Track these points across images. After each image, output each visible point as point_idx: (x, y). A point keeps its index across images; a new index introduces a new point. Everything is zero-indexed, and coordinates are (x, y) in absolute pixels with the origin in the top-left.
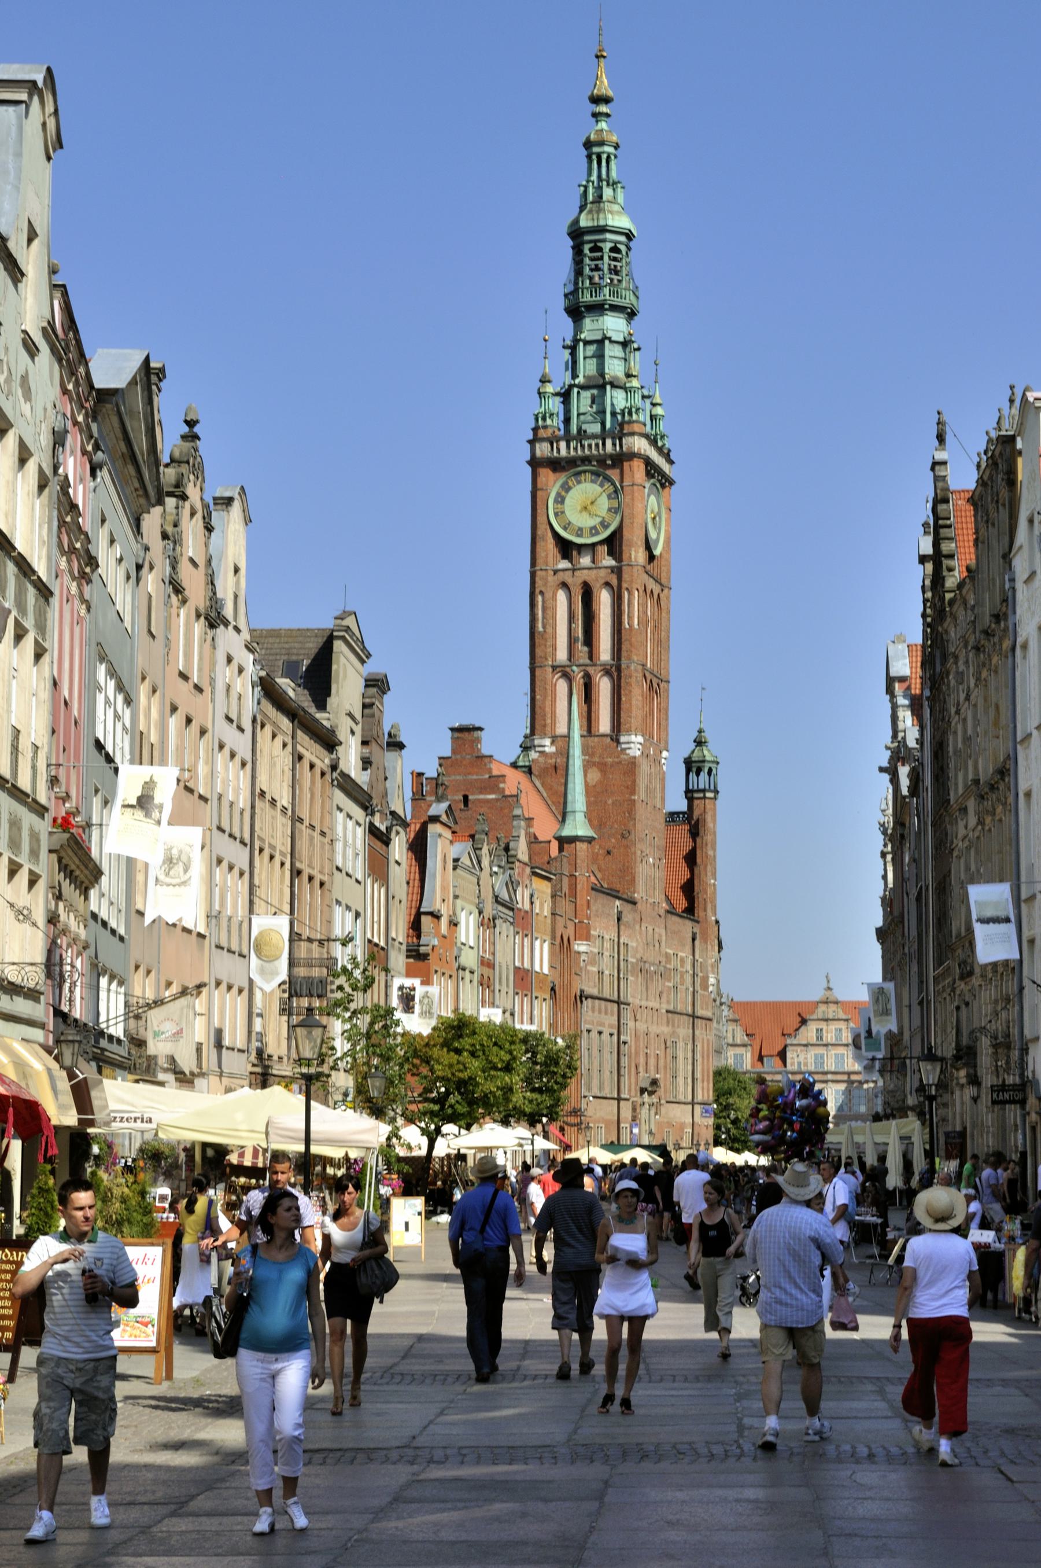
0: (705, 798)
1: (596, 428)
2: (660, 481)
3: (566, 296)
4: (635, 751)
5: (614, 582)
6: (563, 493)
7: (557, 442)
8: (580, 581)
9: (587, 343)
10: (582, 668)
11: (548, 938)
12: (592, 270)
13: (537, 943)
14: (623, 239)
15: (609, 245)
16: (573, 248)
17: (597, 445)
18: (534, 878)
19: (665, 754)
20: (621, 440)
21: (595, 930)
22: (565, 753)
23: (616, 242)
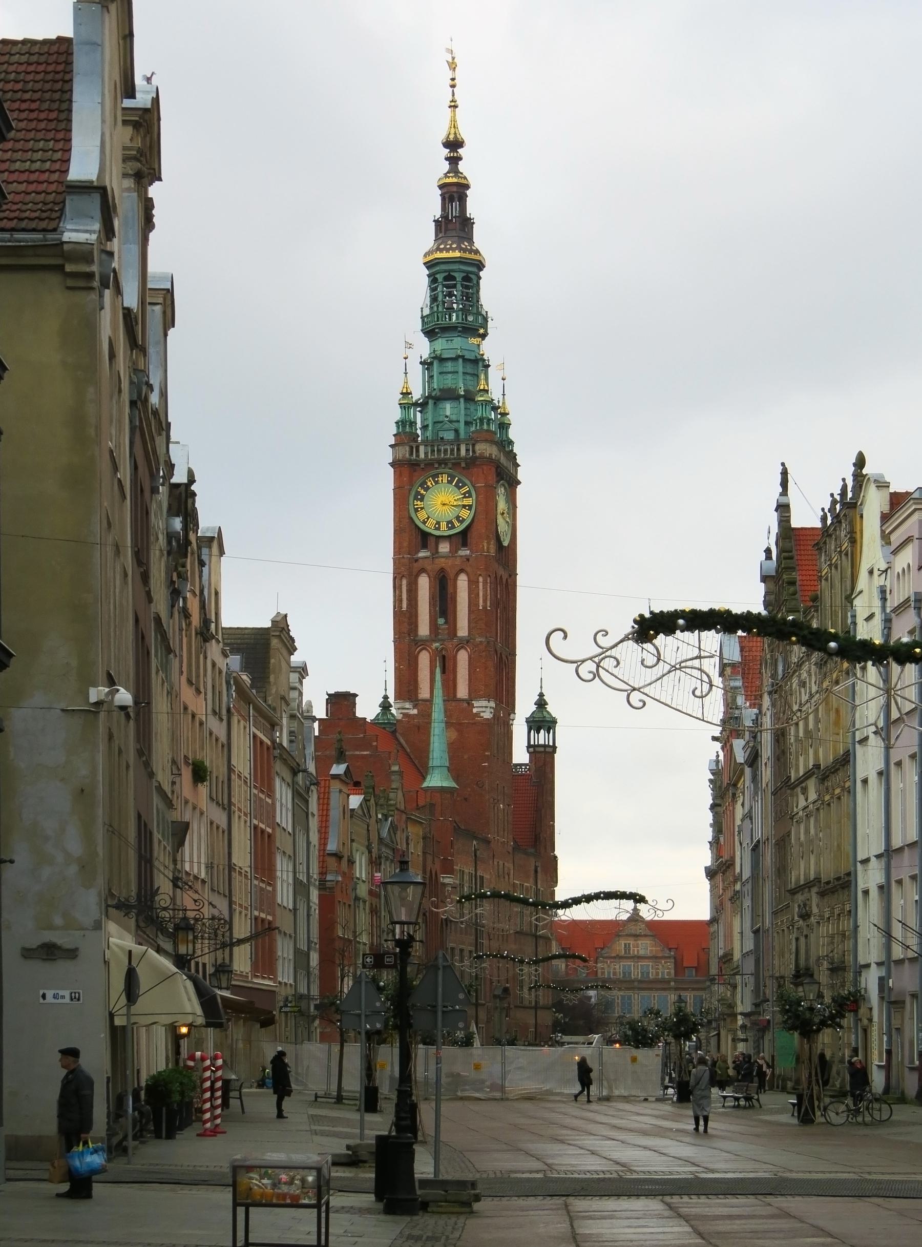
0: (545, 752)
1: (449, 436)
3: (423, 317)
4: (487, 715)
5: (468, 569)
6: (422, 492)
8: (438, 567)
9: (442, 360)
14: (474, 269)
16: (429, 276)
17: (452, 450)
19: (512, 716)
20: (474, 445)
22: (426, 715)
23: (468, 272)
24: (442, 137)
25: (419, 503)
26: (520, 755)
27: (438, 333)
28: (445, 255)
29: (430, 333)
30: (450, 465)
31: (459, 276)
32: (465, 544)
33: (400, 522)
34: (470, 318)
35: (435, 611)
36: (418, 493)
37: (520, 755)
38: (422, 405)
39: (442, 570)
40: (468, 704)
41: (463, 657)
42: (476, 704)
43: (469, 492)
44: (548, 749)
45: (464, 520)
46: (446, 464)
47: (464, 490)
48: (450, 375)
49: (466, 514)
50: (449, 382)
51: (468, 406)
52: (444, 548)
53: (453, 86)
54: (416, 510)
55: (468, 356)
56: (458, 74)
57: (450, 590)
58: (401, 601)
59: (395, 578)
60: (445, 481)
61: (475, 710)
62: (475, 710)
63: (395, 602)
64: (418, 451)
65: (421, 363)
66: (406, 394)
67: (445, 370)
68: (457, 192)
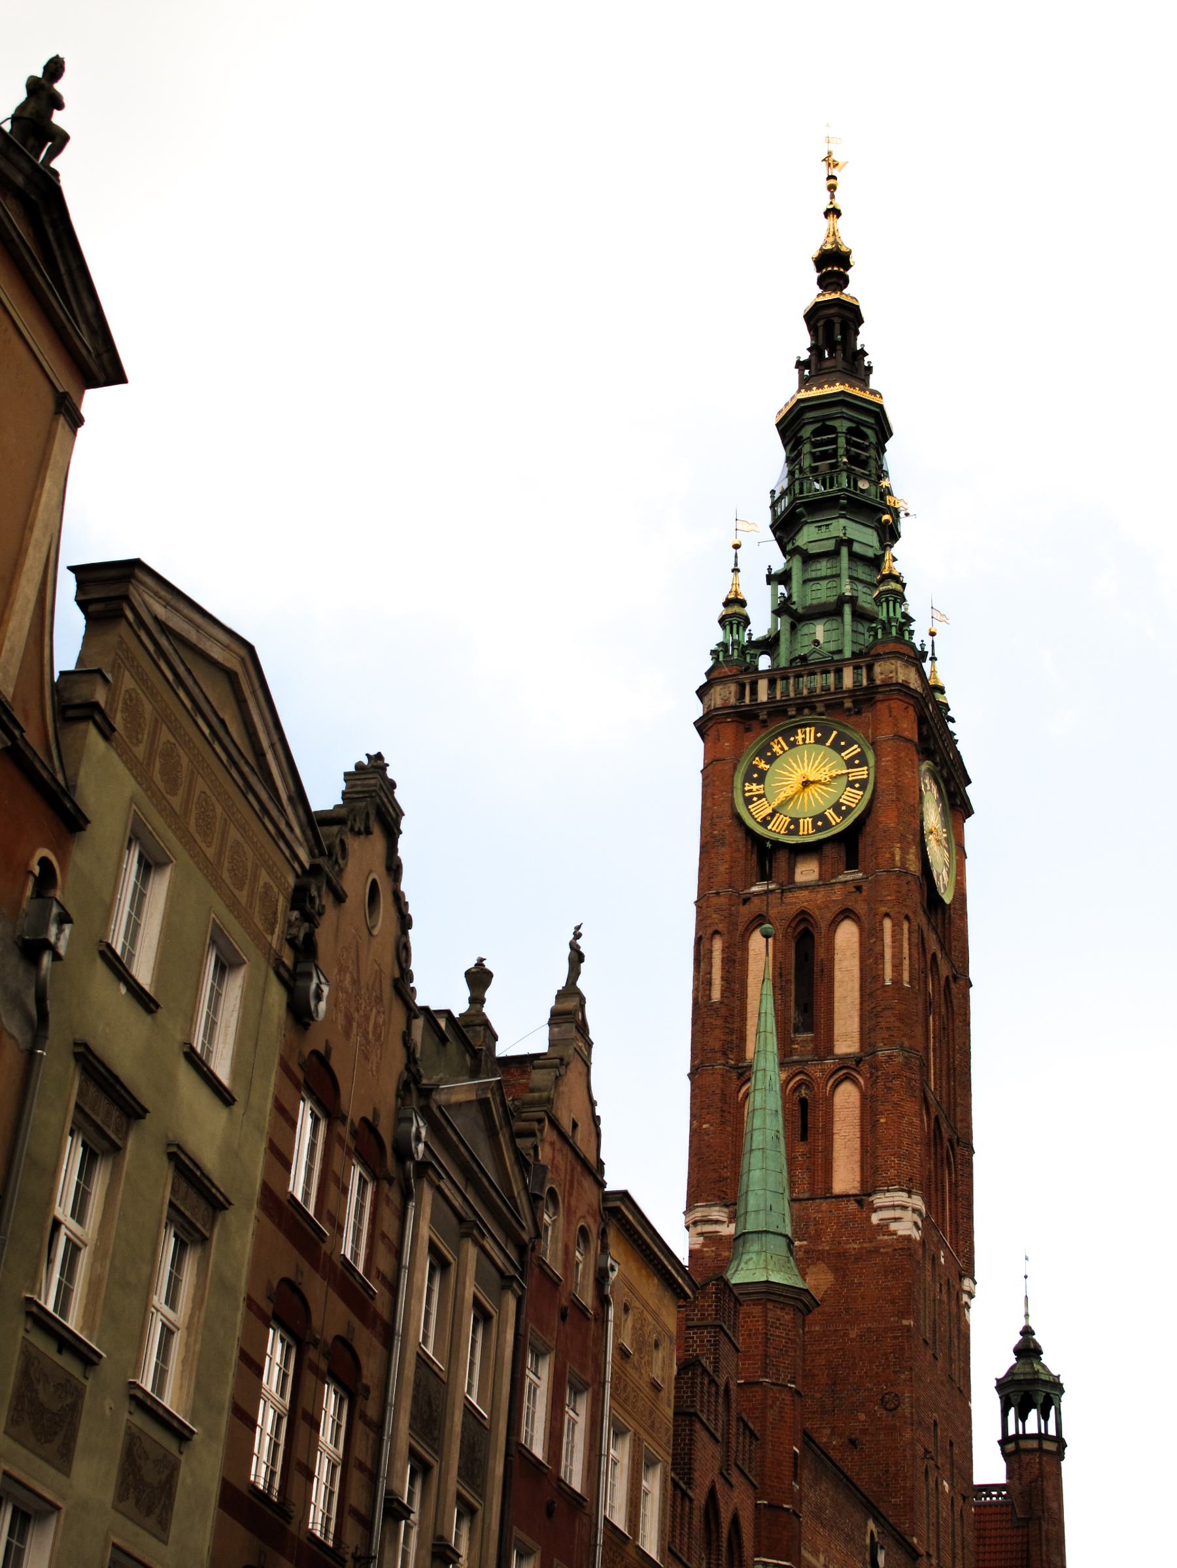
2: (947, 782)
3: (773, 506)
4: (906, 1227)
5: (861, 908)
6: (762, 765)
8: (792, 910)
9: (809, 558)
10: (795, 1069)
11: (665, 1456)
12: (816, 458)
13: (620, 1453)
14: (872, 421)
18: (612, 1236)
19: (967, 1283)
20: (870, 668)
21: (816, 1556)
23: (860, 423)
25: (754, 787)
26: (989, 1467)
27: (801, 515)
28: (815, 392)
29: (785, 527)
30: (820, 708)
31: (842, 426)
32: (852, 863)
33: (713, 825)
35: (785, 1003)
36: (754, 768)
37: (989, 1467)
38: (769, 645)
39: (803, 916)
40: (860, 1203)
41: (847, 1099)
42: (879, 1200)
43: (861, 756)
44: (1049, 1446)
45: (850, 809)
46: (813, 708)
48: (824, 583)
50: (822, 594)
52: (807, 872)
54: (748, 801)
55: (857, 548)
57: (820, 953)
58: (710, 983)
59: (699, 941)
61: (875, 1218)
62: (875, 1218)
63: (696, 990)
64: (754, 692)
66: (735, 602)
67: (814, 575)
68: (839, 315)
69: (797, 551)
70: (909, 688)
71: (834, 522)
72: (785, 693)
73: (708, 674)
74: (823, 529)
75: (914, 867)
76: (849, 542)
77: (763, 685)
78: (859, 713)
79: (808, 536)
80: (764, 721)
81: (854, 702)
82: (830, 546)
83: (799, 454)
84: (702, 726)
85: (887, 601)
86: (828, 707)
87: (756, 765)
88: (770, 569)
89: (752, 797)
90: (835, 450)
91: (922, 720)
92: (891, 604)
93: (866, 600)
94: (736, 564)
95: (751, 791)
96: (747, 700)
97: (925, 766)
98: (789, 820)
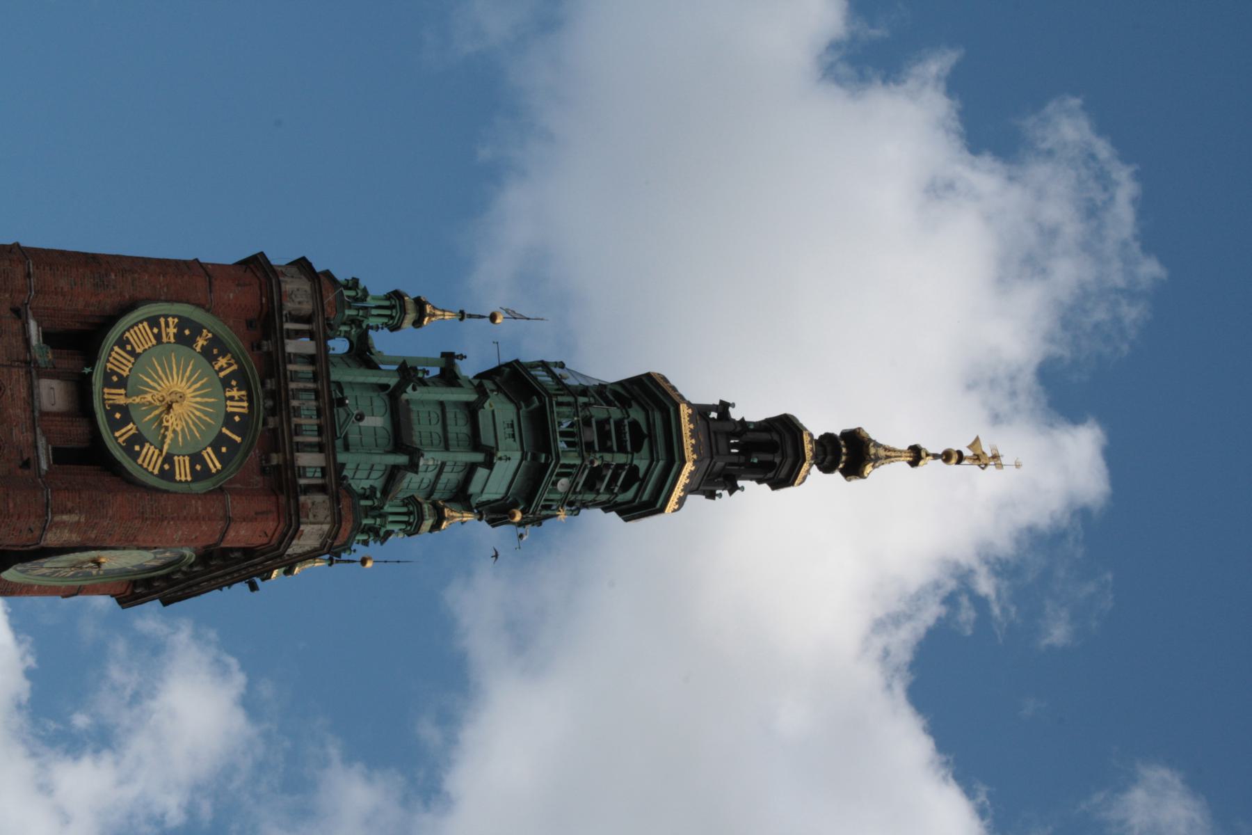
2: (166, 578)
3: (544, 365)
6: (201, 342)
7: (311, 335)
9: (472, 411)
12: (602, 424)
14: (645, 497)
15: (642, 464)
17: (298, 430)
20: (322, 489)
23: (643, 482)
24: (877, 432)
25: (172, 330)
27: (528, 404)
28: (687, 427)
29: (514, 379)
30: (272, 422)
32: (61, 456)
34: (563, 484)
36: (197, 330)
38: (362, 354)
45: (135, 456)
46: (273, 412)
47: (209, 455)
49: (150, 459)
50: (424, 427)
51: (375, 475)
52: (53, 394)
53: (946, 456)
54: (153, 322)
55: (481, 473)
56: (968, 468)
60: (232, 407)
64: (298, 334)
65: (449, 357)
67: (450, 415)
69: (483, 394)
70: (292, 538)
71: (517, 445)
72: (295, 377)
73: (327, 274)
74: (509, 431)
75: (51, 539)
76: (489, 465)
77: (305, 346)
78: (263, 471)
79: (501, 412)
80: (259, 347)
81: (278, 466)
82: (486, 438)
83: (609, 403)
84: (256, 264)
85: (408, 514)
86: (274, 430)
87: (200, 334)
88: (462, 357)
89: (159, 327)
90: (610, 450)
91: (249, 552)
92: (405, 518)
93: (413, 483)
94: (470, 316)
95: (167, 325)
96: (289, 326)
97: (189, 553)
98: (125, 374)
